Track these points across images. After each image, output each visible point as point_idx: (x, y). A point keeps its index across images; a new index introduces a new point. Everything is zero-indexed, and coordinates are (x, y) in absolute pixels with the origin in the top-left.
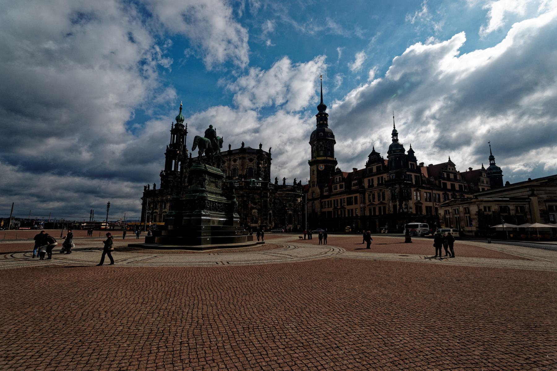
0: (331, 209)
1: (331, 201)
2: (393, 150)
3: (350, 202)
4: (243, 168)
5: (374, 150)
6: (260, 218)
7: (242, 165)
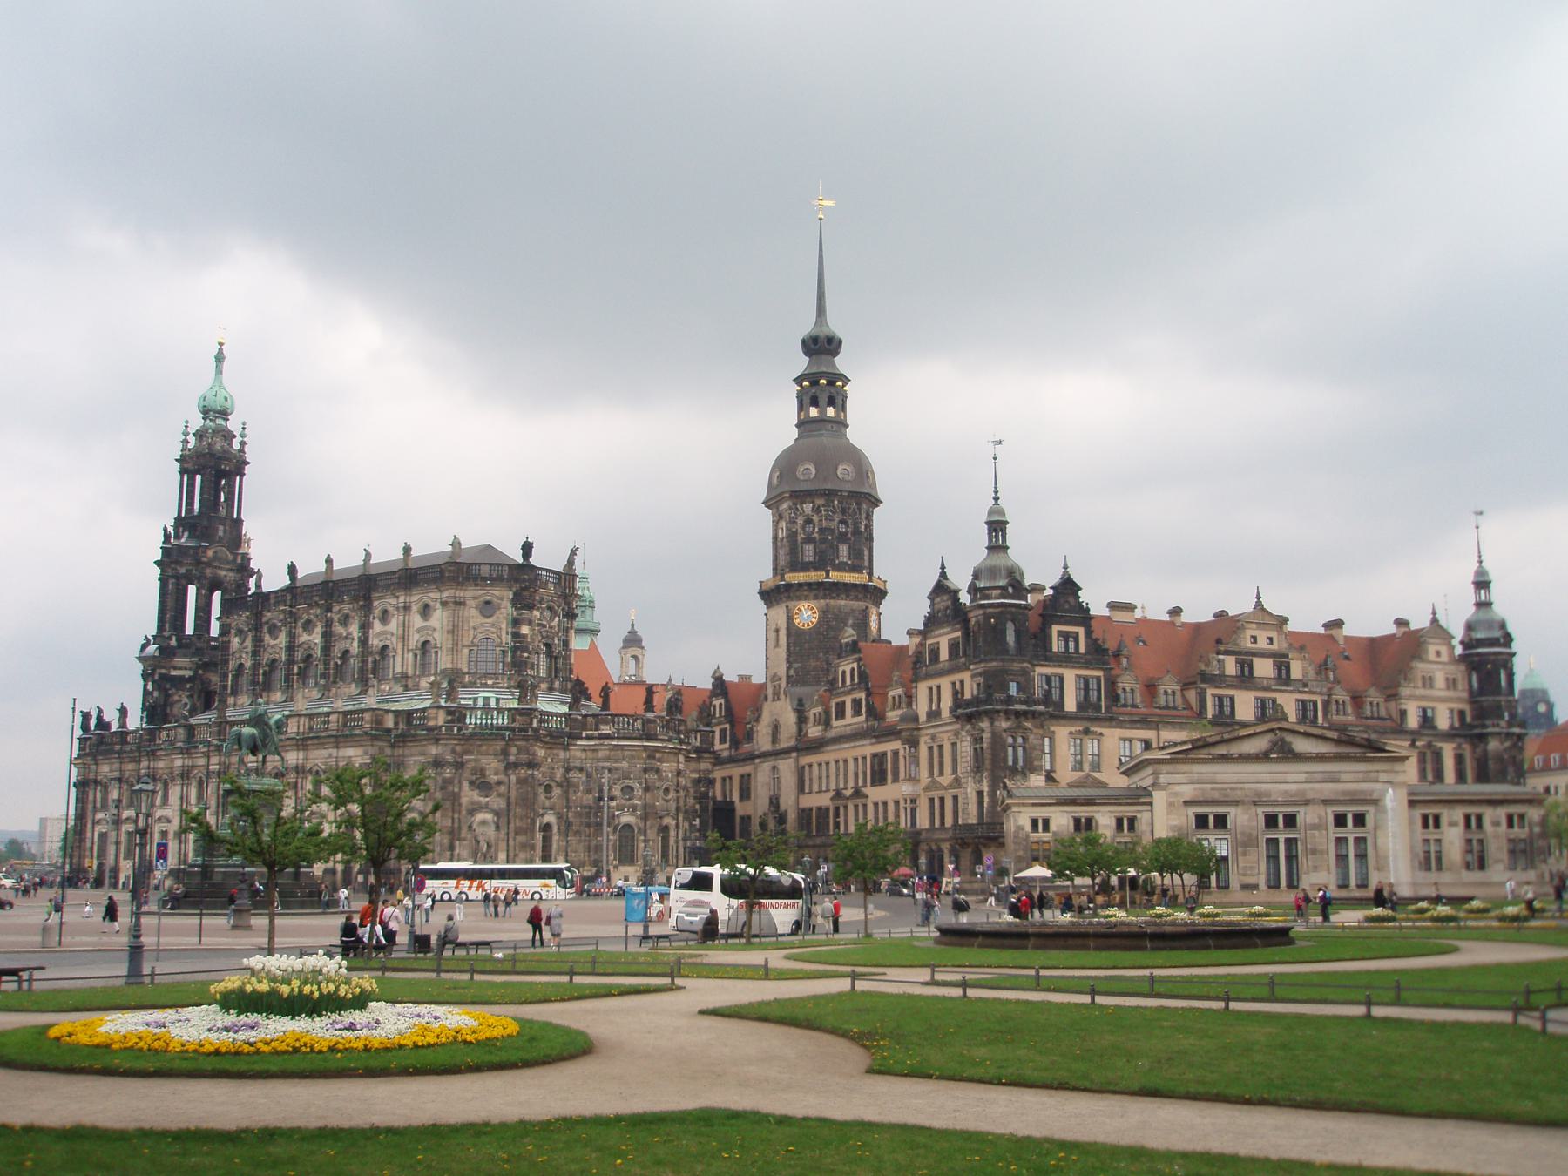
0: (824, 800)
4: (455, 644)
5: (943, 575)
6: (503, 845)
7: (453, 631)
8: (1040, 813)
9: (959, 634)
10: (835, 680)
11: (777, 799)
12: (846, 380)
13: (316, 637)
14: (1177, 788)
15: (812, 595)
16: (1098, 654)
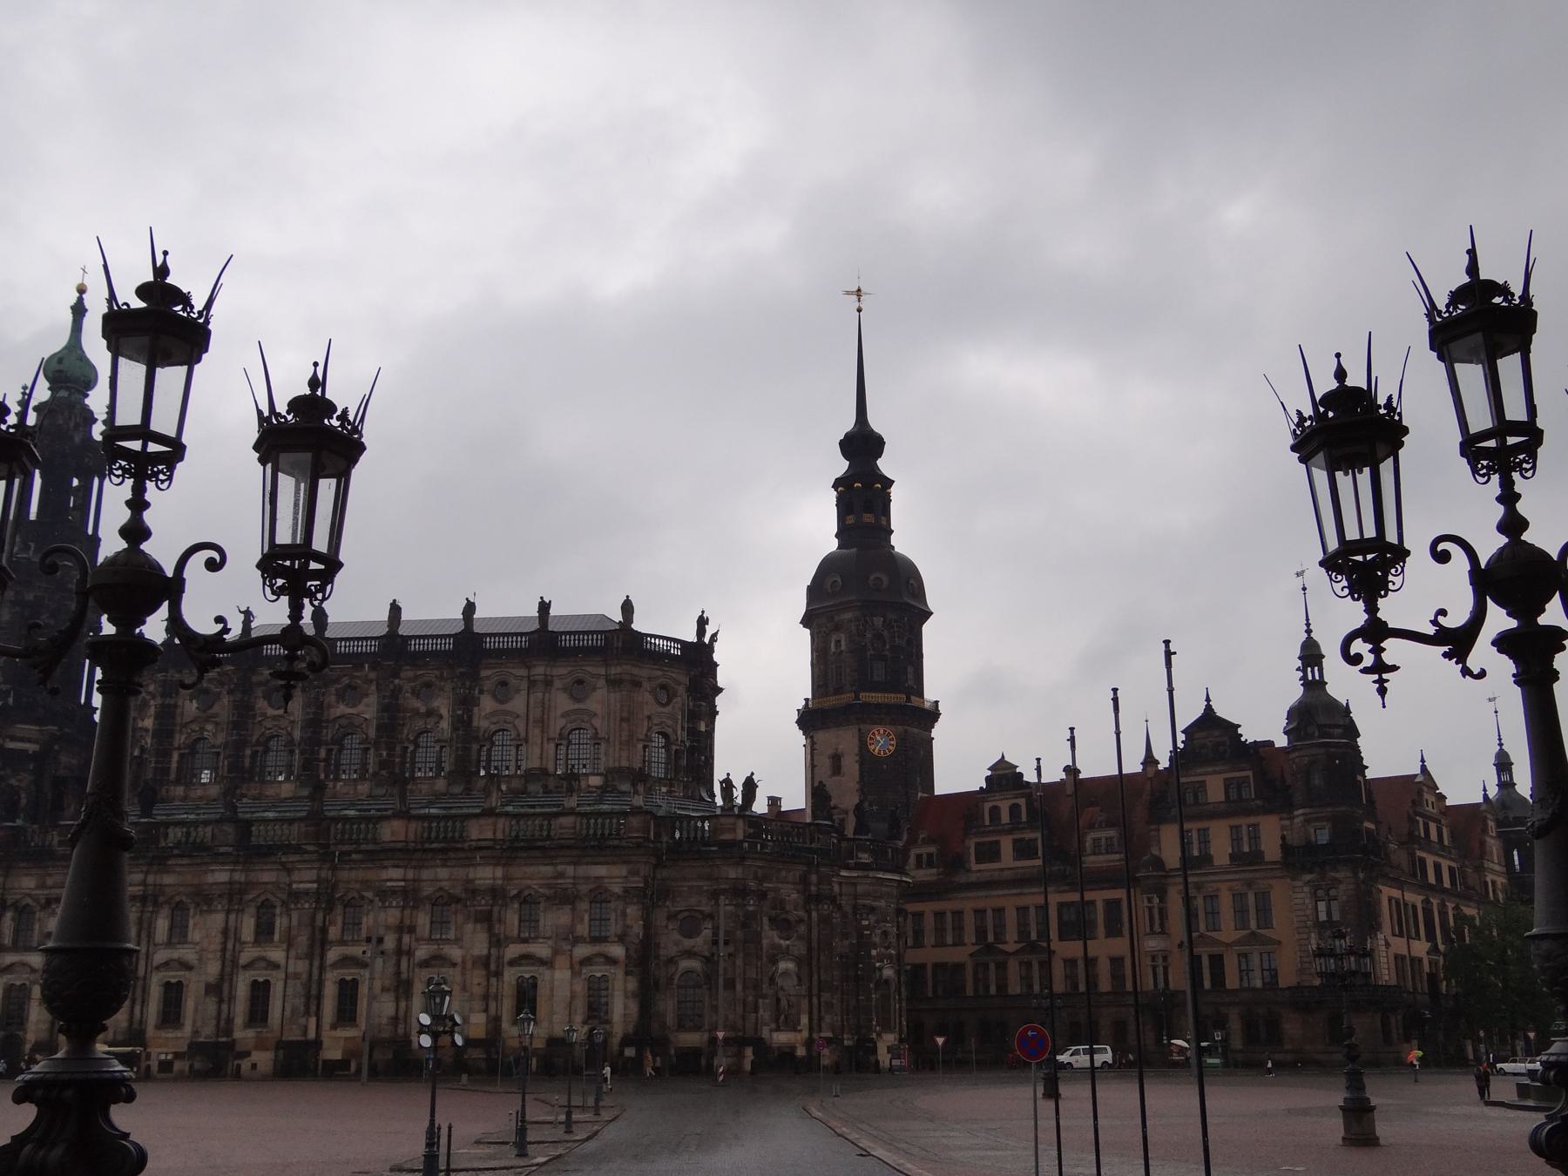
0: (960, 955)
1: (958, 914)
2: (1320, 727)
3: (1077, 925)
5: (1209, 708)
6: (805, 1004)
9: (1250, 773)
13: (368, 709)
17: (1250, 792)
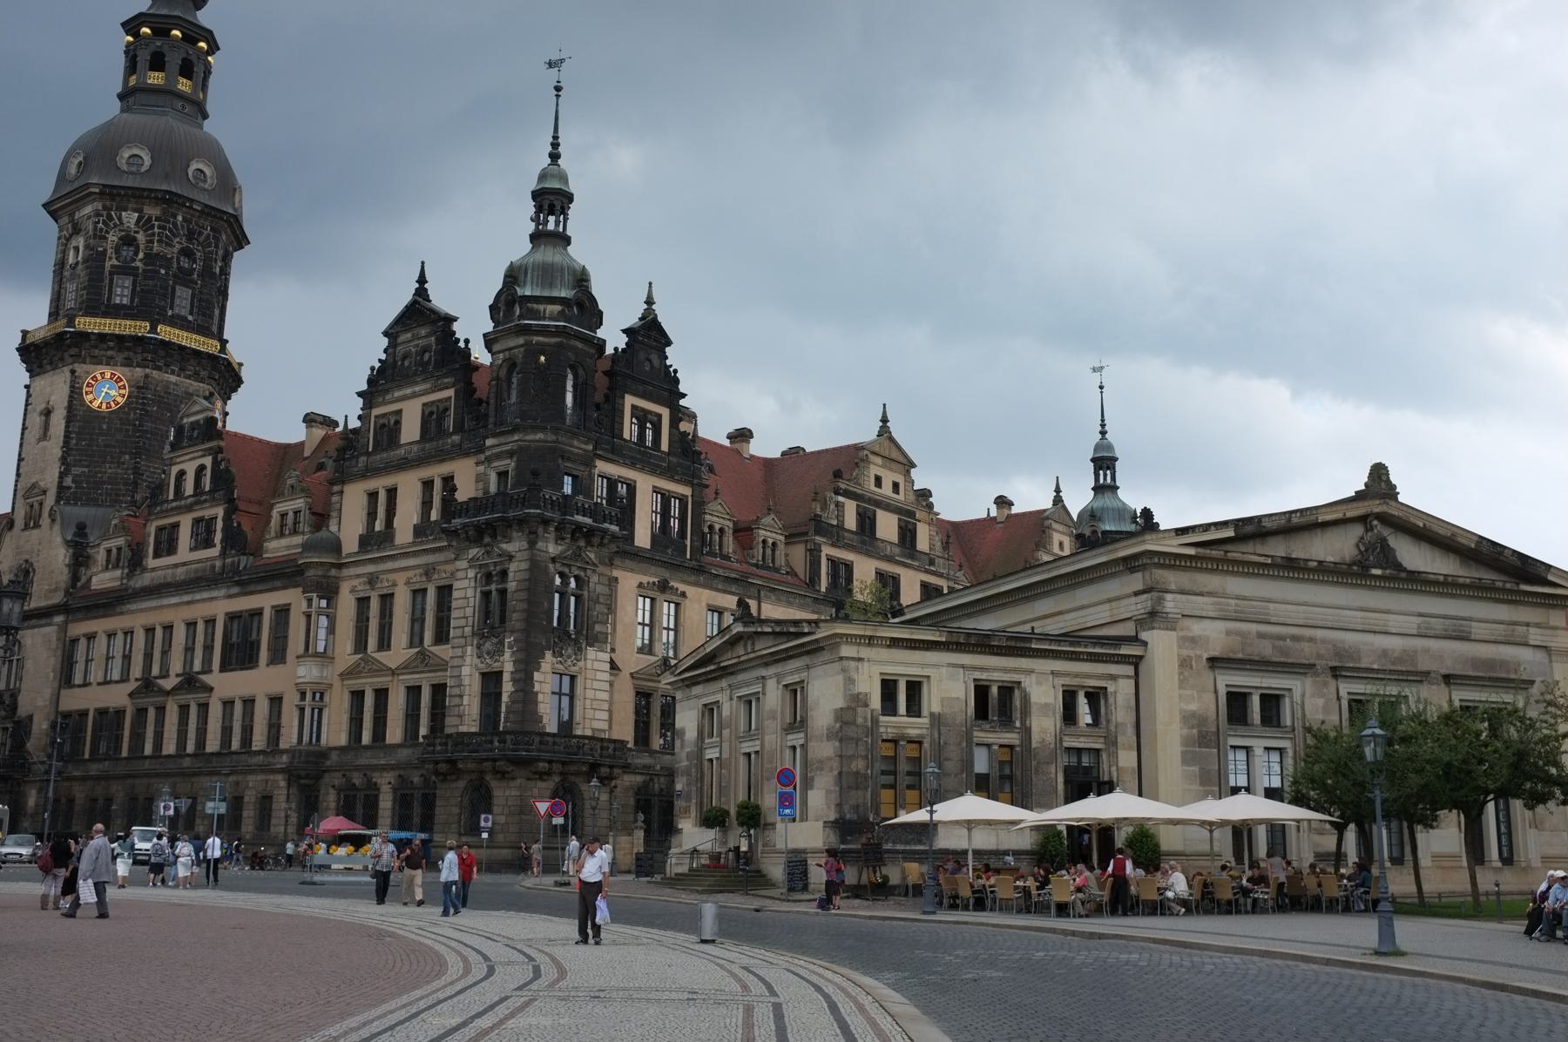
0: (117, 697)
1: (129, 633)
5: (421, 292)
8: (905, 664)
9: (450, 393)
10: (160, 487)
11: (14, 695)
12: (214, 48)
14: (1197, 628)
15: (120, 358)
16: (688, 456)
17: (450, 423)
